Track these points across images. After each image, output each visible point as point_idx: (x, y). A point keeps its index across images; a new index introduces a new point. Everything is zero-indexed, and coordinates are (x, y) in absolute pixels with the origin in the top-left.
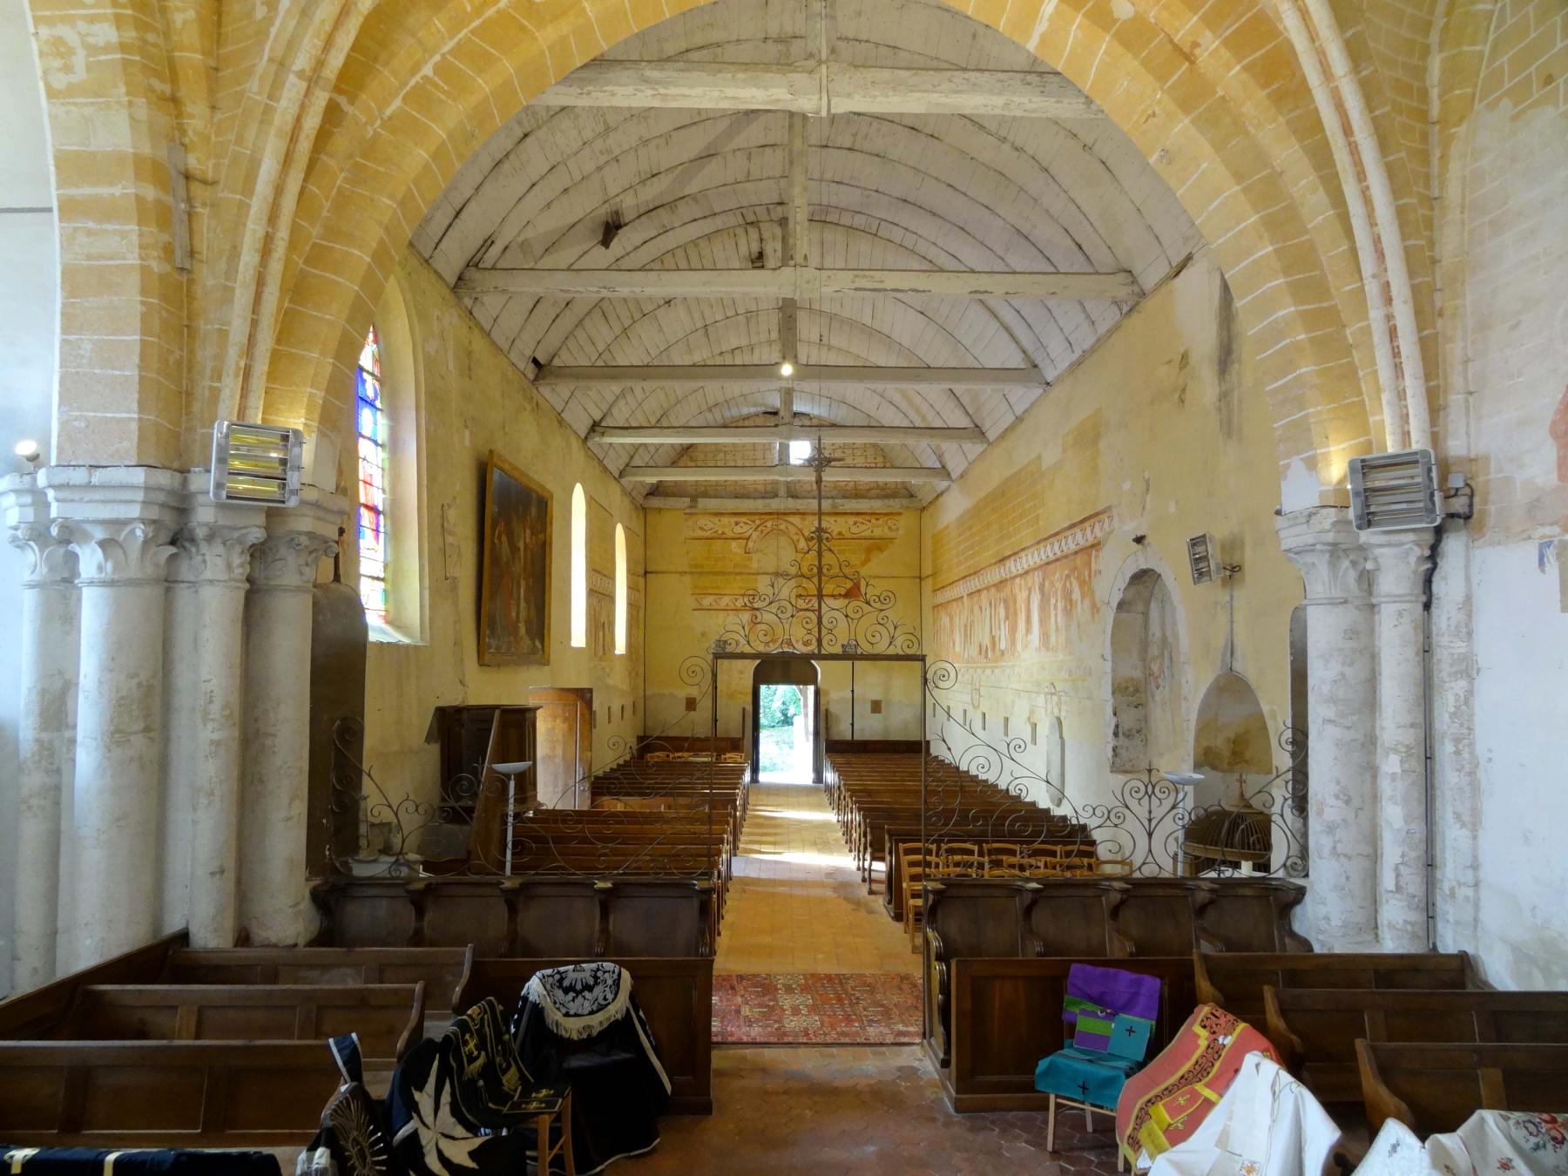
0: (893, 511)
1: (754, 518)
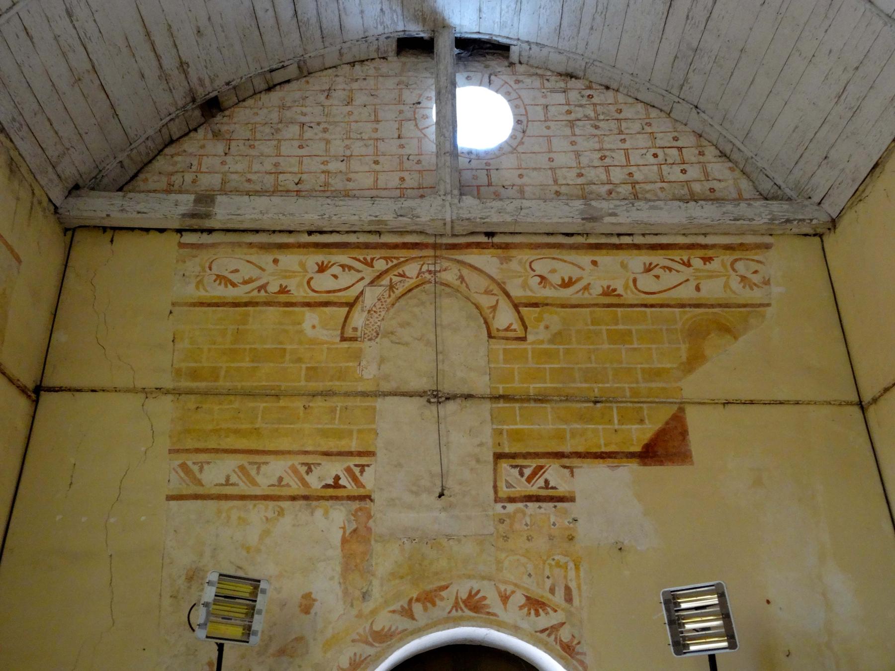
0: (749, 239)
1: (369, 255)
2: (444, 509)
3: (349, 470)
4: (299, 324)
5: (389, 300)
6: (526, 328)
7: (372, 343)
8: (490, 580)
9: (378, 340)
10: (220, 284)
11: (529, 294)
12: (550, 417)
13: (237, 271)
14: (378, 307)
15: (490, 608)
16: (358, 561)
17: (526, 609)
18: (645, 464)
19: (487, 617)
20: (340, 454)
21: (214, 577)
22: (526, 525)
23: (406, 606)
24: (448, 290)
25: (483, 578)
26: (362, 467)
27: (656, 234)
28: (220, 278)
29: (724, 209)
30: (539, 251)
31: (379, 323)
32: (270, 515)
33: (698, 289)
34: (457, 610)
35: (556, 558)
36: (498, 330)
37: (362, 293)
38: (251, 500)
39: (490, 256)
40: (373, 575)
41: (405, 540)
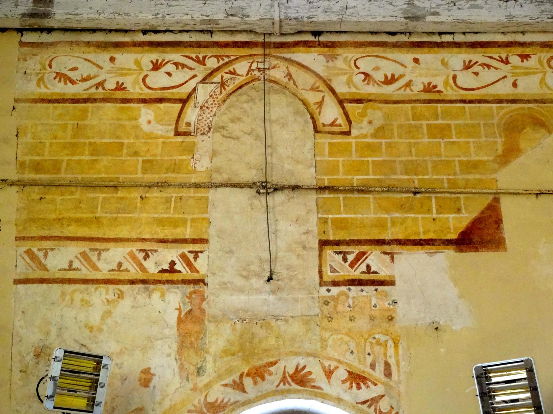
1: (202, 53)
2: (273, 292)
3: (183, 256)
4: (136, 119)
5: (220, 97)
6: (350, 122)
7: (205, 137)
8: (315, 357)
9: (210, 134)
10: (60, 81)
11: (354, 90)
12: (372, 207)
13: (75, 69)
14: (210, 103)
15: (315, 382)
16: (193, 339)
17: (349, 383)
18: (461, 251)
19: (313, 390)
20: (175, 241)
21: (60, 354)
22: (349, 306)
23: (237, 380)
24: (276, 87)
25: (309, 355)
26: (196, 254)
27: (476, 33)
28: (60, 76)
29: (543, 8)
30: (363, 49)
31: (211, 119)
32: (111, 297)
33: (515, 85)
34: (284, 384)
35: (377, 336)
36: (324, 125)
37: (194, 90)
38: (93, 283)
39: (316, 54)
40: (206, 352)
41: (236, 320)
